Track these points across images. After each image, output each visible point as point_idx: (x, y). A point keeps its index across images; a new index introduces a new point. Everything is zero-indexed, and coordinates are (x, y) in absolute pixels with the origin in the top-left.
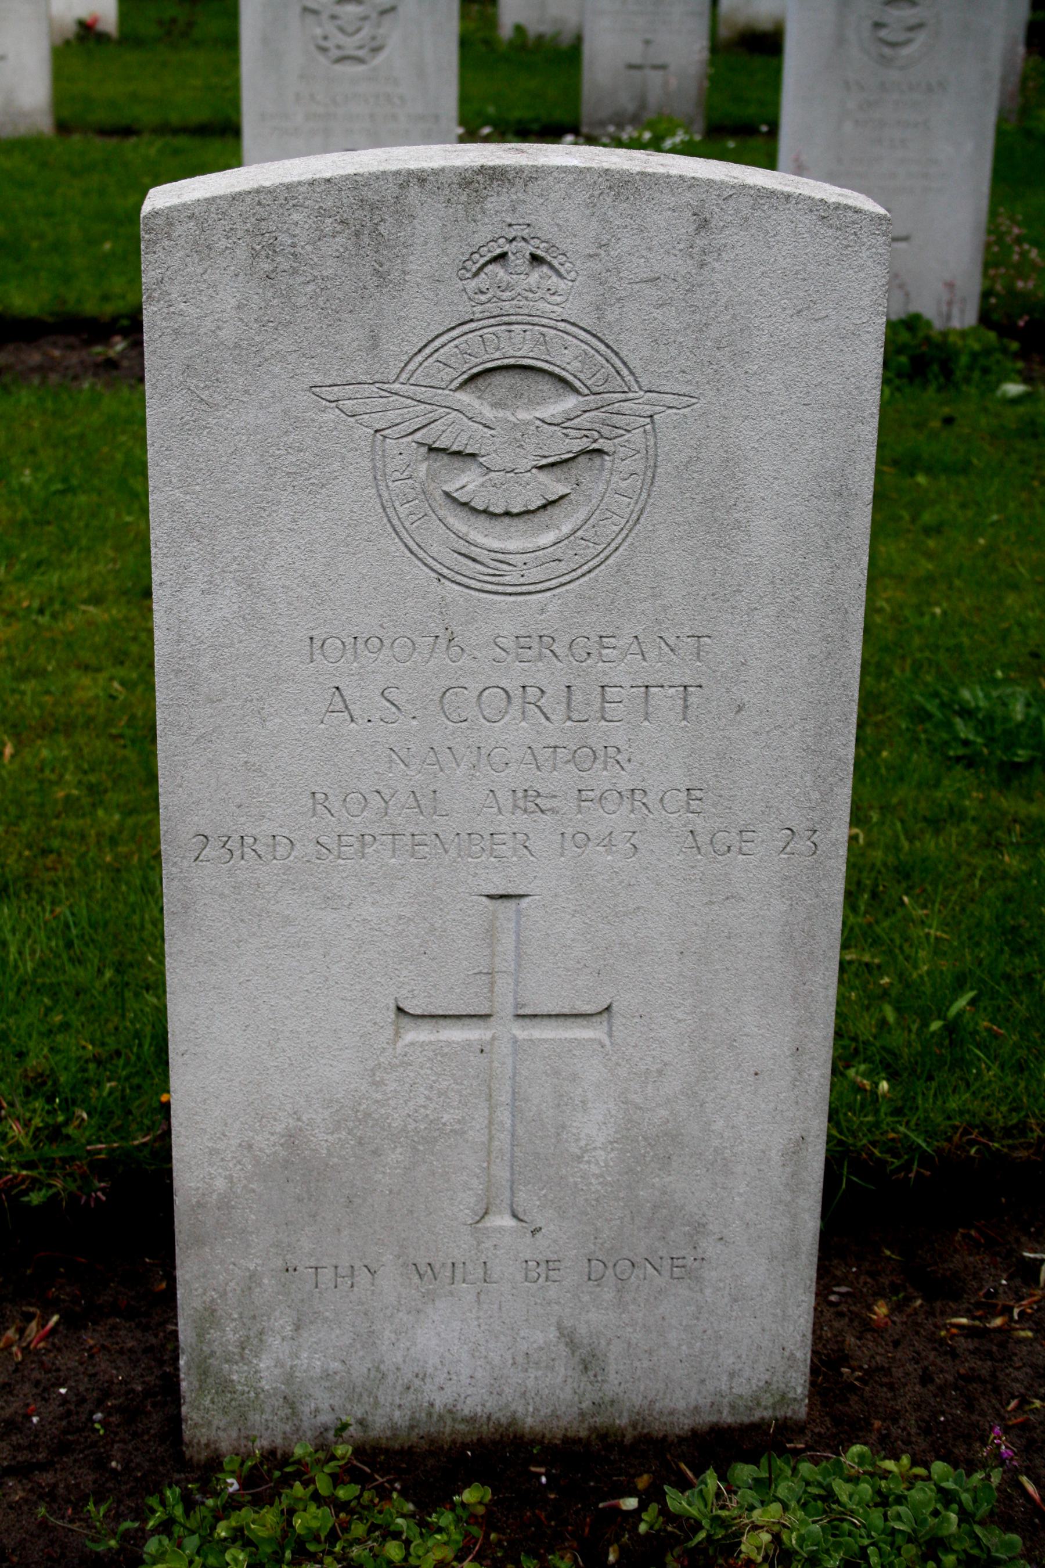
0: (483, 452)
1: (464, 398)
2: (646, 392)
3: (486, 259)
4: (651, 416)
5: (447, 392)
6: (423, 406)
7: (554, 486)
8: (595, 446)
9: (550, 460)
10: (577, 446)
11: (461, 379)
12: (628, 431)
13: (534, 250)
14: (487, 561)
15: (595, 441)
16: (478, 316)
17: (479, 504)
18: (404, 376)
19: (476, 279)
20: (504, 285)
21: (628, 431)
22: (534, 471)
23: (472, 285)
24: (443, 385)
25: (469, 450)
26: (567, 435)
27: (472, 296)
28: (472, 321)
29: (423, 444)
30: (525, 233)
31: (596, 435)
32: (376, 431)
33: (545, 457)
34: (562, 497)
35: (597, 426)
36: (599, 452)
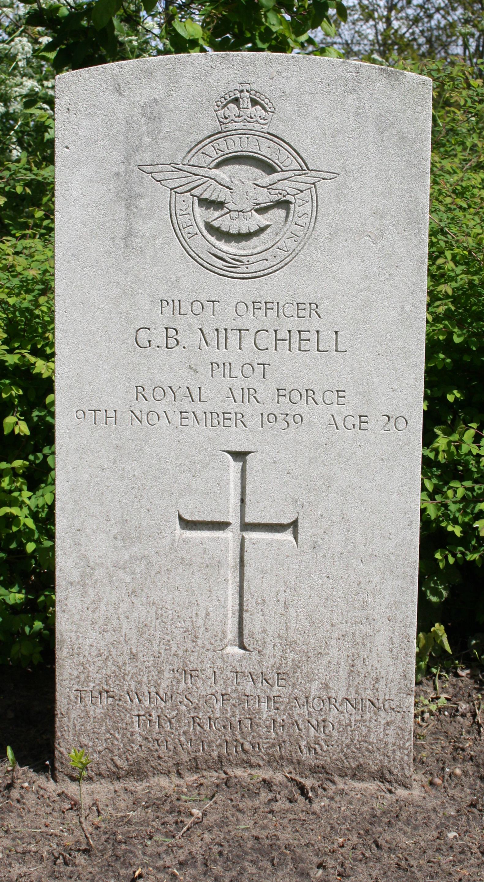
2: (312, 170)
4: (314, 184)
5: (206, 169)
6: (194, 177)
7: (262, 220)
8: (284, 198)
9: (262, 205)
10: (276, 198)
12: (302, 191)
14: (227, 259)
15: (284, 196)
17: (224, 228)
19: (222, 111)
20: (237, 115)
21: (302, 191)
22: (253, 211)
23: (220, 113)
27: (222, 120)
28: (220, 133)
30: (248, 87)
31: (285, 193)
32: (171, 189)
33: (259, 204)
34: (268, 226)
36: (288, 203)
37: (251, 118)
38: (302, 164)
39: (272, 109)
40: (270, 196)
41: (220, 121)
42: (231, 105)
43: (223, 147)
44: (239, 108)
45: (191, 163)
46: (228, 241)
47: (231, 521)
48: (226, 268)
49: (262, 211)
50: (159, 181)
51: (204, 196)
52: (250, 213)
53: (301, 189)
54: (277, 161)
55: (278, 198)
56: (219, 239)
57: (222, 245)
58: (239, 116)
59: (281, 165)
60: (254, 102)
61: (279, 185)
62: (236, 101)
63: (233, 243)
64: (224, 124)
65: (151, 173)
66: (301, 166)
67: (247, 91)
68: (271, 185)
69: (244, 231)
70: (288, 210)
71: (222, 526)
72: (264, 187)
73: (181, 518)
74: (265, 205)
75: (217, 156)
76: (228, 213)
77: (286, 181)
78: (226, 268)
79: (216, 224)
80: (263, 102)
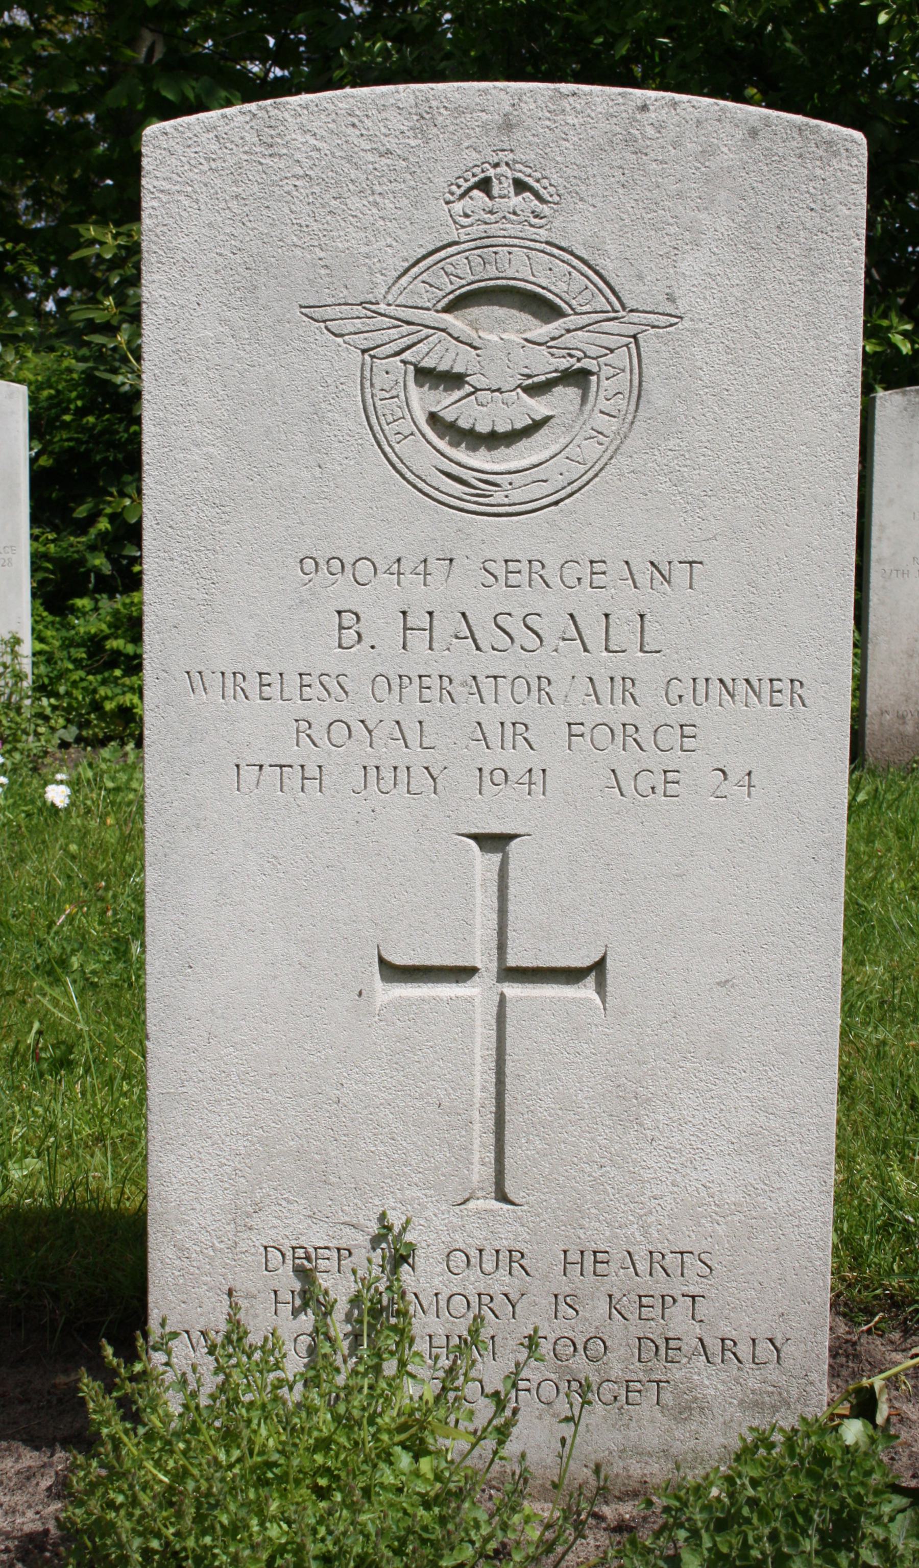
0: (469, 372)
1: (448, 318)
2: (632, 311)
3: (469, 184)
4: (634, 337)
5: (432, 312)
6: (406, 329)
8: (578, 365)
9: (536, 379)
10: (564, 363)
11: (446, 300)
12: (612, 351)
13: (519, 175)
15: (579, 360)
16: (463, 238)
17: (464, 424)
18: (390, 298)
19: (462, 202)
21: (612, 351)
22: (519, 390)
23: (458, 207)
24: (429, 305)
25: (454, 371)
26: (552, 355)
29: (411, 363)
31: (579, 354)
34: (547, 419)
35: (580, 346)
37: (515, 213)
38: (613, 299)
39: (556, 198)
40: (552, 360)
41: (455, 222)
42: (476, 193)
43: (463, 269)
44: (491, 197)
45: (401, 300)
46: (473, 448)
47: (479, 965)
48: (468, 498)
49: (536, 389)
50: (341, 336)
51: (428, 363)
52: (514, 393)
53: (612, 346)
54: (564, 295)
55: (568, 365)
56: (454, 444)
57: (460, 454)
58: (491, 212)
59: (574, 303)
60: (520, 186)
61: (568, 340)
62: (484, 185)
63: (483, 451)
64: (463, 227)
65: (324, 321)
66: (610, 303)
67: (507, 164)
68: (553, 339)
69: (503, 427)
70: (584, 387)
71: (463, 973)
72: (540, 344)
73: (382, 961)
74: (543, 378)
75: (451, 288)
76: (473, 393)
77: (579, 333)
78: (468, 498)
79: (449, 415)
80: (536, 185)
